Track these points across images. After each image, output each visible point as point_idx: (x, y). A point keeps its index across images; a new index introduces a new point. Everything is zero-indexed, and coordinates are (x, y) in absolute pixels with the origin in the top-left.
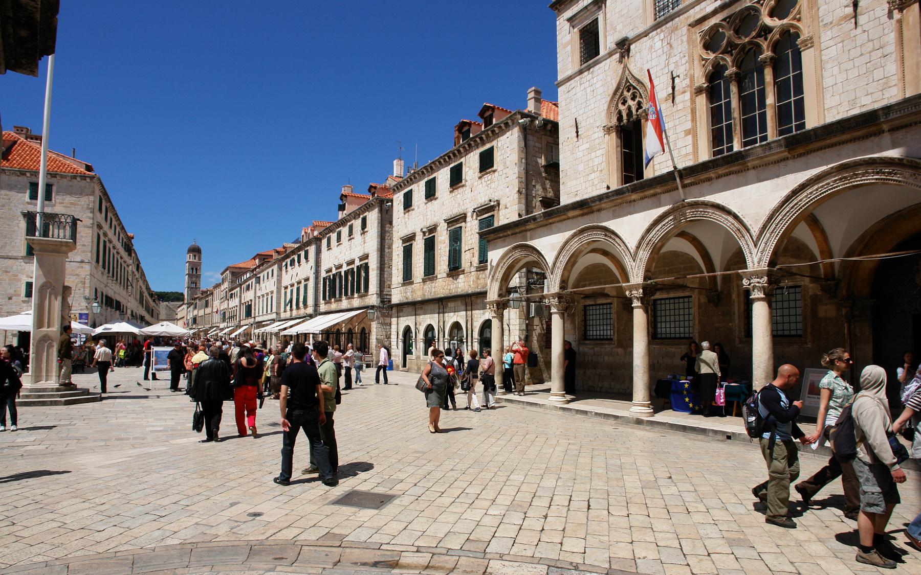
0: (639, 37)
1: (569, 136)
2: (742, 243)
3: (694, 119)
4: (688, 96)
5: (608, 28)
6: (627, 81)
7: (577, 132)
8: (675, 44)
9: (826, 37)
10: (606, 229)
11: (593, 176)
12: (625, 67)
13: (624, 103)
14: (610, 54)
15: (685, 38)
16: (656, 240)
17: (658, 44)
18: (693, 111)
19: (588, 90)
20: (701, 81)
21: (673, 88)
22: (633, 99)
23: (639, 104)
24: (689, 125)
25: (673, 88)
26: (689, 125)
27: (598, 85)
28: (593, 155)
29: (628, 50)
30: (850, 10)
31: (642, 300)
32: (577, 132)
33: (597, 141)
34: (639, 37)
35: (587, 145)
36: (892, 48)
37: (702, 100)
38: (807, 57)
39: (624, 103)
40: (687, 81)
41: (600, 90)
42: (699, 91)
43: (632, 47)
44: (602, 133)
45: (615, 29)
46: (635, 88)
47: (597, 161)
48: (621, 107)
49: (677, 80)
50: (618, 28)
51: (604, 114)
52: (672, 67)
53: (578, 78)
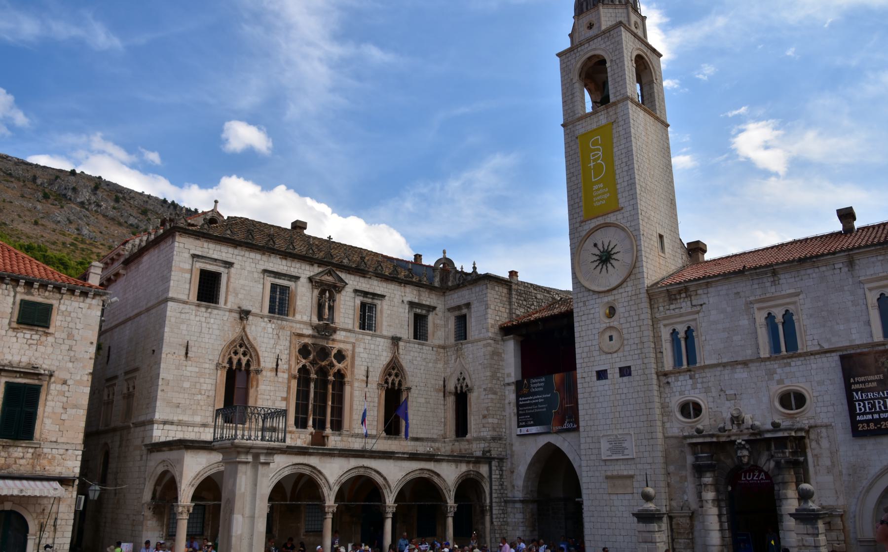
0: (256, 315)
1: (176, 352)
2: (385, 491)
3: (288, 392)
4: (286, 376)
5: (231, 289)
6: (242, 339)
7: (187, 353)
8: (281, 338)
9: (356, 384)
10: (314, 468)
11: (199, 397)
12: (244, 329)
13: (236, 353)
14: (231, 311)
15: (288, 338)
16: (343, 481)
17: (270, 330)
18: (289, 388)
19: (204, 325)
20: (295, 372)
21: (277, 365)
22: (244, 354)
23: (248, 361)
24: (285, 395)
25: (277, 365)
26: (285, 395)
27: (215, 327)
28: (202, 380)
29: (247, 319)
30: (365, 378)
31: (333, 513)
32: (187, 353)
33: (207, 371)
34: (256, 315)
35: (197, 370)
36: (376, 405)
37: (294, 384)
38: (347, 389)
39: (236, 353)
40: (286, 367)
41: (217, 332)
42: (295, 377)
43: (250, 318)
44: (213, 367)
45: (237, 294)
46: (246, 347)
47: (205, 387)
48: (233, 355)
49: (279, 362)
50: (240, 296)
51: (217, 353)
52: (278, 351)
53: (193, 307)
